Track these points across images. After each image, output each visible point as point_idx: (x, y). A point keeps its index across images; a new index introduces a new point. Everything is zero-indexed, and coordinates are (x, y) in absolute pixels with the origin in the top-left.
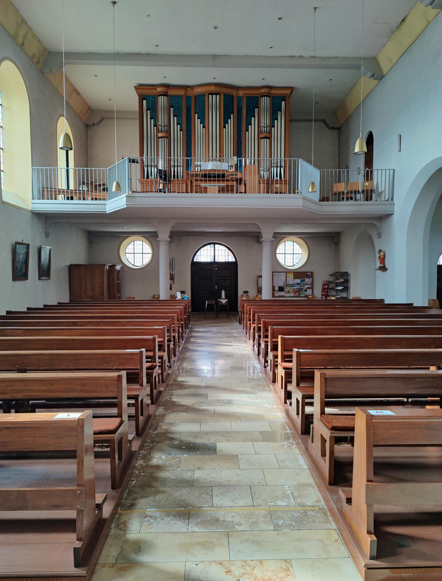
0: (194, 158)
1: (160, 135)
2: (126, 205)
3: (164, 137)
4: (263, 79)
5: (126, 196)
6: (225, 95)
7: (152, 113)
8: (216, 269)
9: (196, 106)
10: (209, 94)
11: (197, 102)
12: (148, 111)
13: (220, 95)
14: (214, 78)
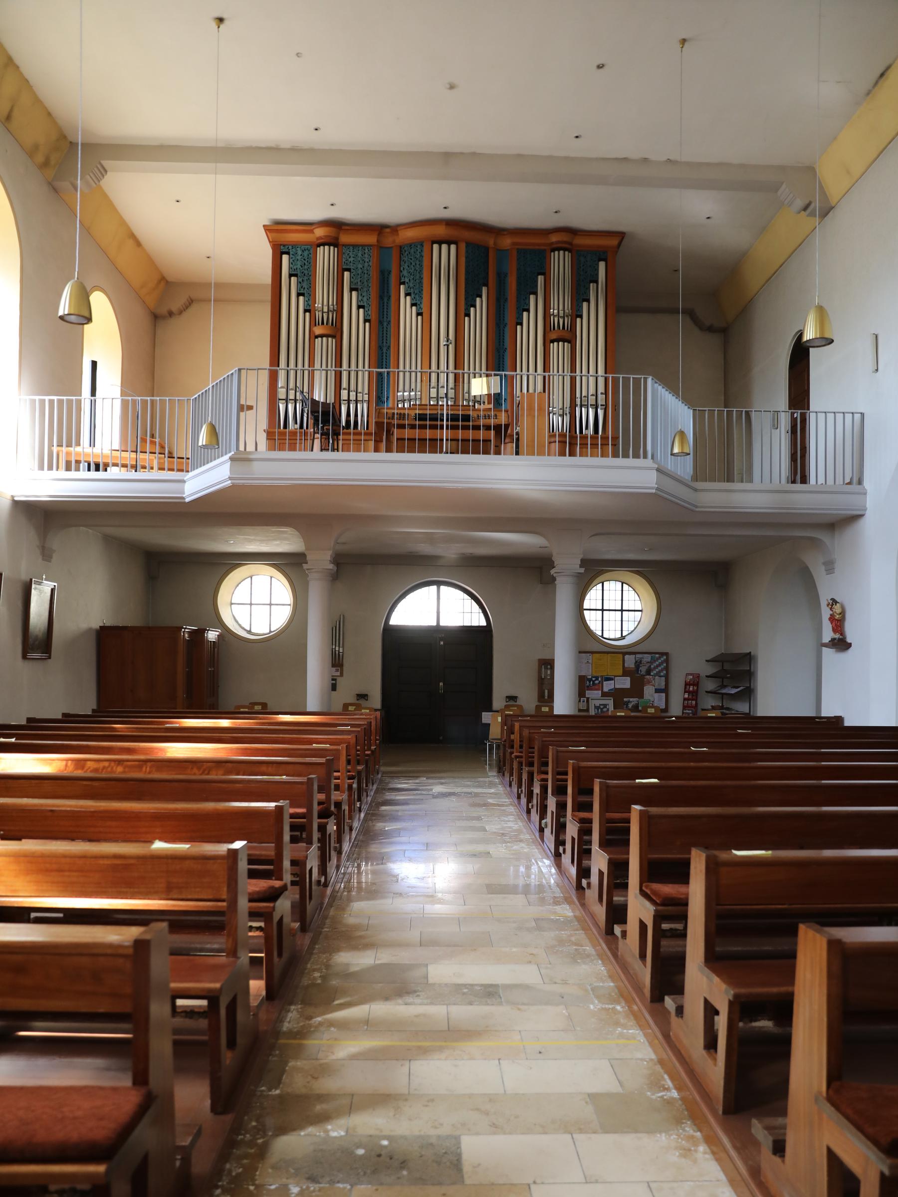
0: (397, 370)
1: (318, 330)
2: (230, 478)
3: (327, 336)
4: (556, 212)
5: (231, 459)
6: (468, 244)
7: (300, 283)
8: (442, 643)
9: (402, 269)
10: (433, 242)
11: (406, 259)
12: (293, 278)
13: (459, 245)
14: (445, 208)
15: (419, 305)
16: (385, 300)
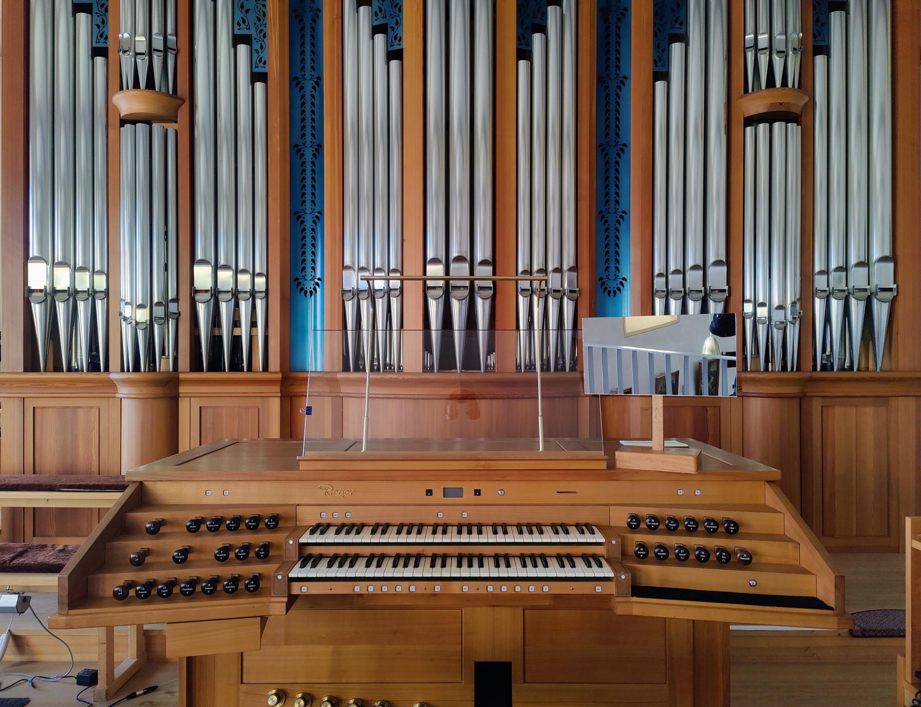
15: (393, 28)
16: (308, 23)
